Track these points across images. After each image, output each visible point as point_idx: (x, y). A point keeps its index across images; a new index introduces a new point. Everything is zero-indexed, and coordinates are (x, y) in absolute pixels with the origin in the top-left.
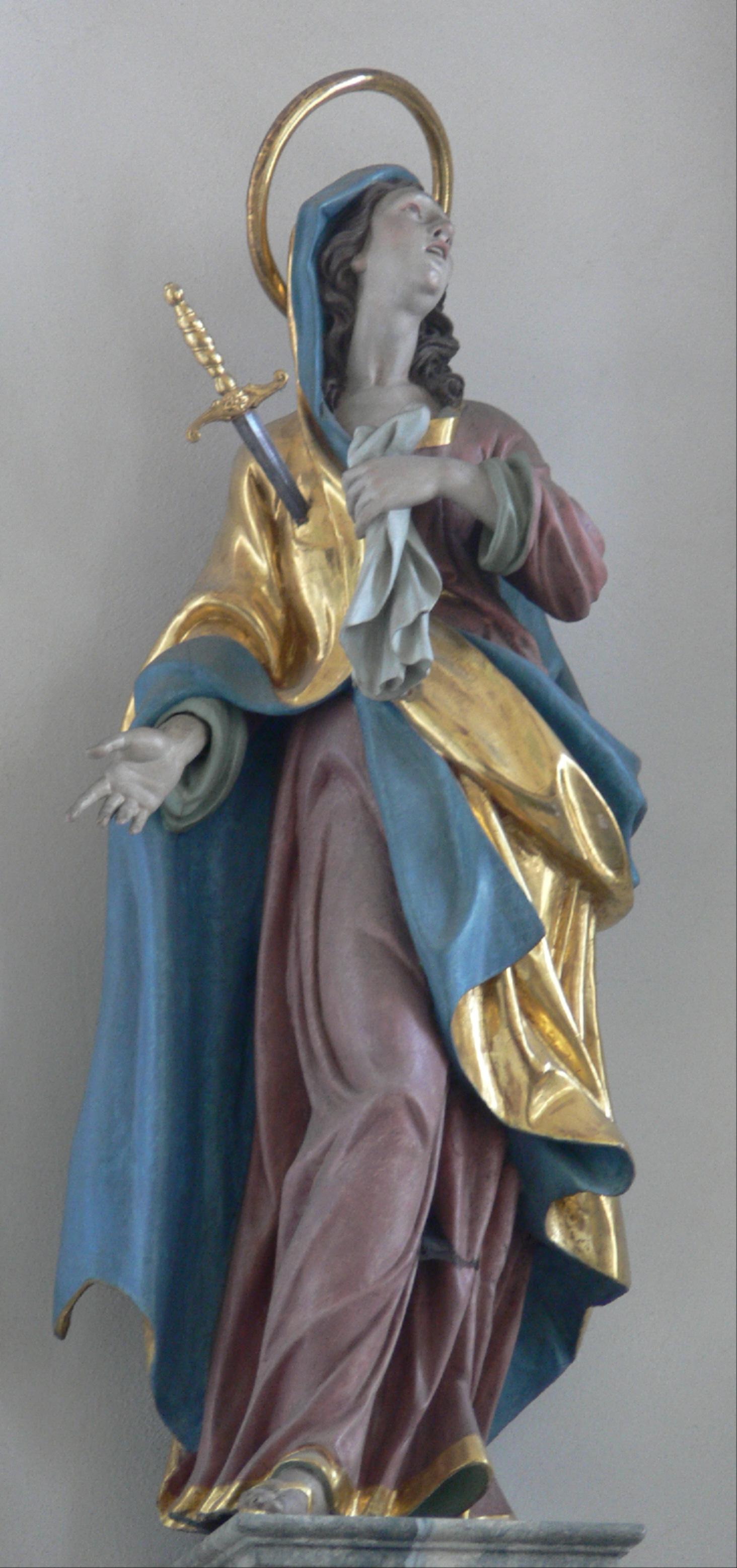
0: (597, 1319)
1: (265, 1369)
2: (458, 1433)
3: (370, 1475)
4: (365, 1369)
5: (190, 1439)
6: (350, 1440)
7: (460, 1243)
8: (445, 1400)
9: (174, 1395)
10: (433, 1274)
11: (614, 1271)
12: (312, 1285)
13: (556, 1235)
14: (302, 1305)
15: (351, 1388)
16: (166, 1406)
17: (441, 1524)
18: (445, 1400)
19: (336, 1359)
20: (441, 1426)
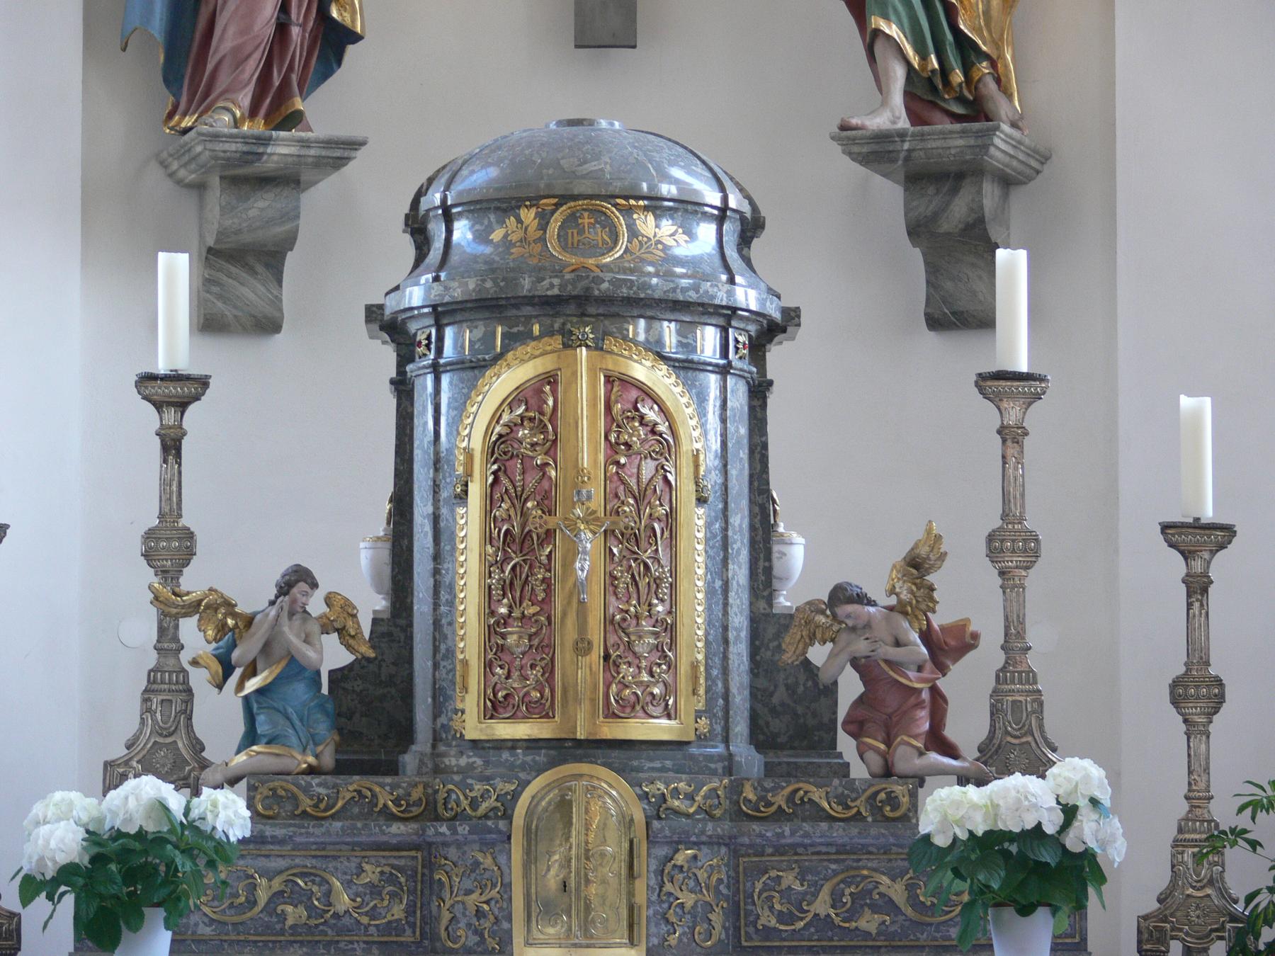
0: (351, 49)
1: (210, 67)
2: (291, 96)
3: (253, 113)
4: (252, 68)
5: (177, 96)
6: (245, 98)
7: (294, 16)
8: (286, 82)
9: (171, 77)
10: (282, 29)
11: (359, 30)
12: (231, 31)
13: (335, 14)
14: (226, 40)
15: (246, 75)
16: (167, 81)
17: (283, 134)
18: (286, 82)
19: (240, 63)
20: (283, 93)
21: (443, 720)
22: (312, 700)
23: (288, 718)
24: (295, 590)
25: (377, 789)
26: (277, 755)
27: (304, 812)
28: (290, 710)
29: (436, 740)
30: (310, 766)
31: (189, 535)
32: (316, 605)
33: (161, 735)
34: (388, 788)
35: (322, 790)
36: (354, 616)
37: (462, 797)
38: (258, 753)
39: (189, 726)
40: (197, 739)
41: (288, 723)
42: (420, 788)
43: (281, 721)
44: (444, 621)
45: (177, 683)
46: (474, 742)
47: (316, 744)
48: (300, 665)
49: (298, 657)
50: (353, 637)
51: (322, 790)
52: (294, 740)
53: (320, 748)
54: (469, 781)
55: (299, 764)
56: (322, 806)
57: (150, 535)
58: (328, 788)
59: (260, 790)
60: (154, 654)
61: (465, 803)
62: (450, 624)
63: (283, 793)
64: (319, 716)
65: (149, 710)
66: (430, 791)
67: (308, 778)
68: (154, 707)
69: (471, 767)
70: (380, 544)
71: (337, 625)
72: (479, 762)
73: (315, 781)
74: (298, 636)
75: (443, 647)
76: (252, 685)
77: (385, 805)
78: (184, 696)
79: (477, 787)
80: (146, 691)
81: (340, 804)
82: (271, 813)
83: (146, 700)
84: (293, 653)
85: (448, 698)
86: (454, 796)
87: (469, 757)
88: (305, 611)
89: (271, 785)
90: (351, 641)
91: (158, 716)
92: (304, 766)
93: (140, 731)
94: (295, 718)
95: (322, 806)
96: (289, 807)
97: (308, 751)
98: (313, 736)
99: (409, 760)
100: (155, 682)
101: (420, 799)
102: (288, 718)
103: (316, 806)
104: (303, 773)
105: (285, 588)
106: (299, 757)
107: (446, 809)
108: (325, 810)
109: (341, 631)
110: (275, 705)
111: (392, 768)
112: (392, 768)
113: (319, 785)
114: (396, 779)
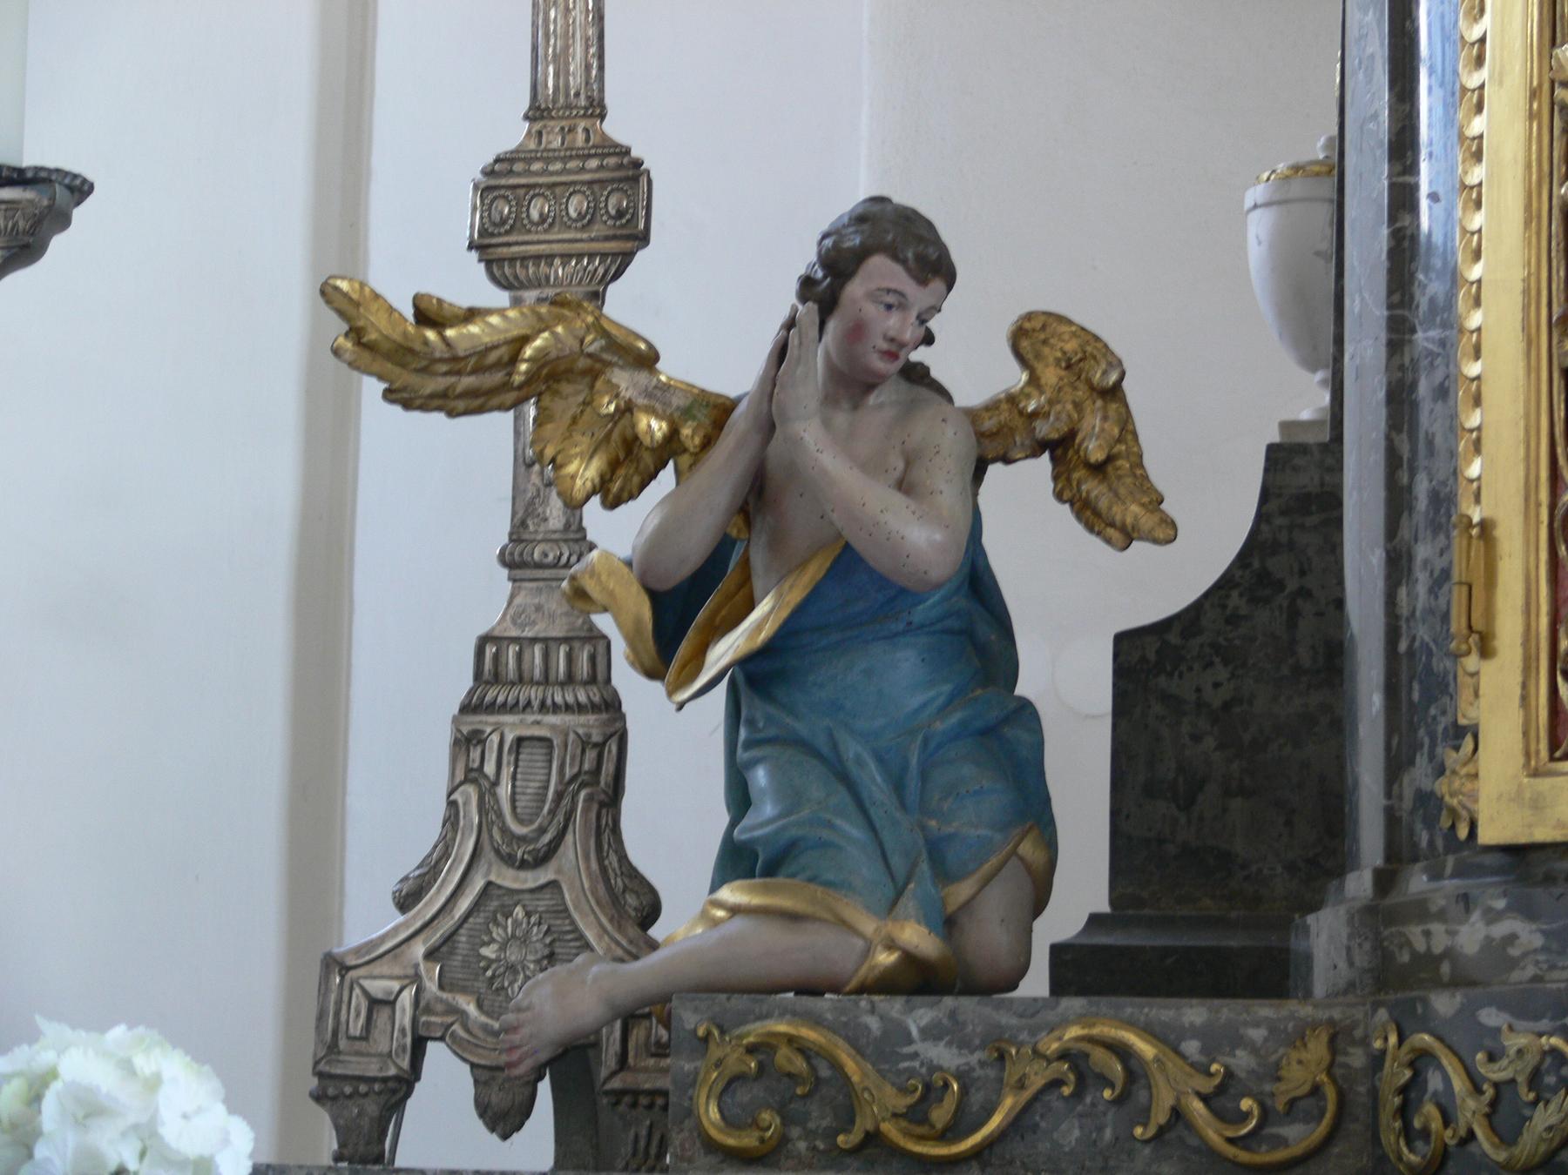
21: (1418, 775)
22: (944, 710)
23: (844, 778)
24: (855, 289)
25: (1146, 1049)
26: (792, 917)
27: (873, 1138)
28: (852, 749)
29: (1398, 855)
30: (910, 959)
31: (630, 174)
32: (971, 359)
33: (508, 860)
34: (1191, 1047)
35: (944, 1055)
36: (1114, 393)
37: (1459, 1084)
38: (735, 910)
39: (607, 832)
40: (633, 874)
41: (842, 796)
42: (1317, 1049)
43: (817, 786)
44: (1424, 388)
45: (570, 679)
46: (1520, 858)
47: (944, 874)
48: (881, 581)
49: (859, 545)
50: (1099, 469)
51: (944, 1055)
52: (862, 865)
53: (962, 891)
54: (1491, 1017)
55: (868, 952)
56: (941, 1115)
57: (501, 182)
58: (964, 1044)
59: (715, 1052)
60: (510, 585)
61: (1470, 1109)
62: (1443, 392)
63: (800, 1064)
64: (967, 770)
65: (473, 775)
66: (1357, 1059)
67: (894, 1006)
68: (490, 769)
69: (1499, 953)
70: (1298, 187)
71: (1044, 429)
72: (1529, 935)
73: (920, 1016)
74: (871, 467)
75: (1422, 487)
76: (725, 651)
77: (1178, 1114)
78: (587, 723)
79: (1513, 1042)
80: (466, 708)
81: (1009, 1104)
82: (749, 1140)
83: (466, 742)
84: (848, 535)
85: (1441, 687)
86: (1434, 1082)
87: (1492, 917)
88: (917, 375)
89: (754, 1031)
90: (1092, 488)
91: (504, 790)
92: (885, 958)
93: (445, 847)
94: (873, 780)
95: (941, 1115)
96: (820, 1119)
97: (908, 903)
98: (936, 850)
99: (1327, 937)
100: (497, 678)
101: (1316, 1090)
102: (844, 778)
103: (916, 1115)
104: (885, 985)
105: (824, 289)
106: (868, 925)
107: (1408, 1133)
108: (952, 1132)
109: (1061, 449)
110: (802, 728)
111: (1274, 974)
112: (1274, 974)
113: (932, 1033)
114: (1228, 1010)
